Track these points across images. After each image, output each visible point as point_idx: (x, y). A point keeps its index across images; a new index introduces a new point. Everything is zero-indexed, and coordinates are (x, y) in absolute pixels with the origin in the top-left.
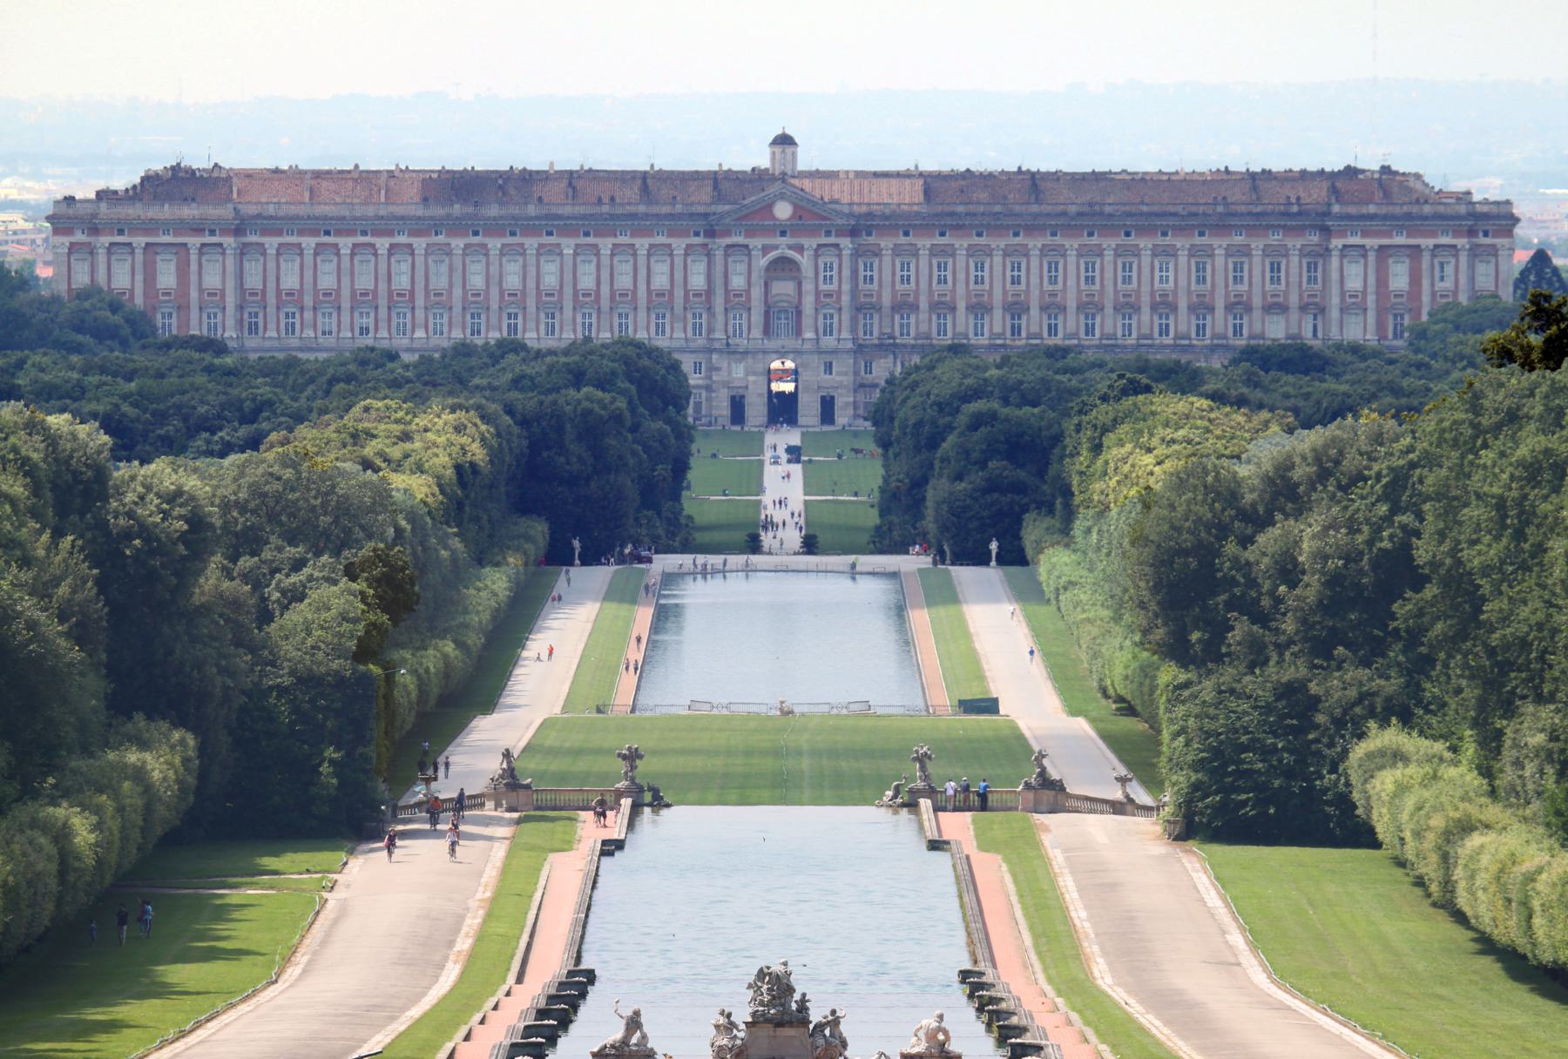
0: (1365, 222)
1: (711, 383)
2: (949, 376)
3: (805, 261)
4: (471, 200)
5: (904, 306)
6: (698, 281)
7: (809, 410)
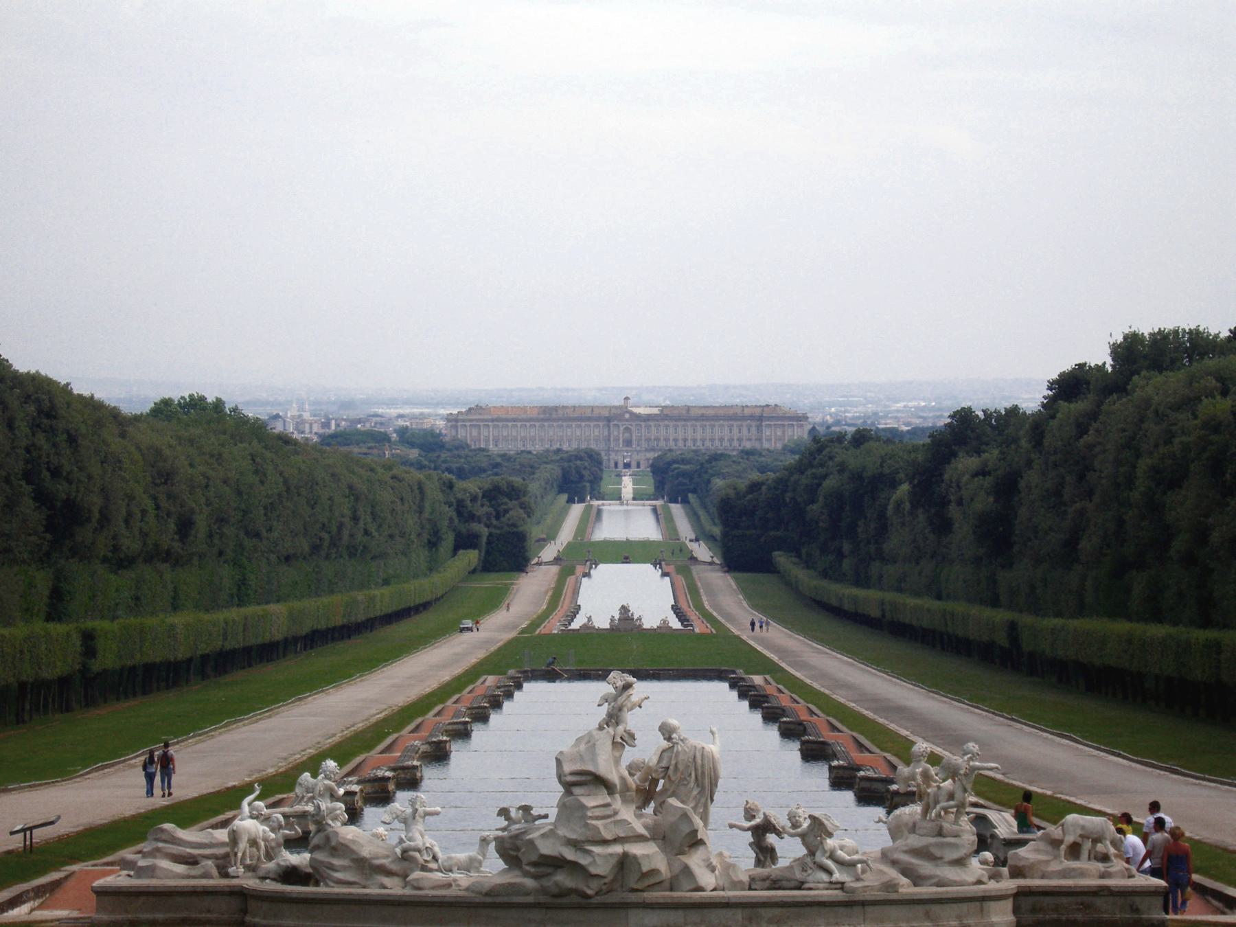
0: (769, 418)
1: (609, 459)
2: (669, 457)
3: (633, 428)
4: (551, 415)
5: (657, 439)
6: (606, 433)
7: (634, 464)
